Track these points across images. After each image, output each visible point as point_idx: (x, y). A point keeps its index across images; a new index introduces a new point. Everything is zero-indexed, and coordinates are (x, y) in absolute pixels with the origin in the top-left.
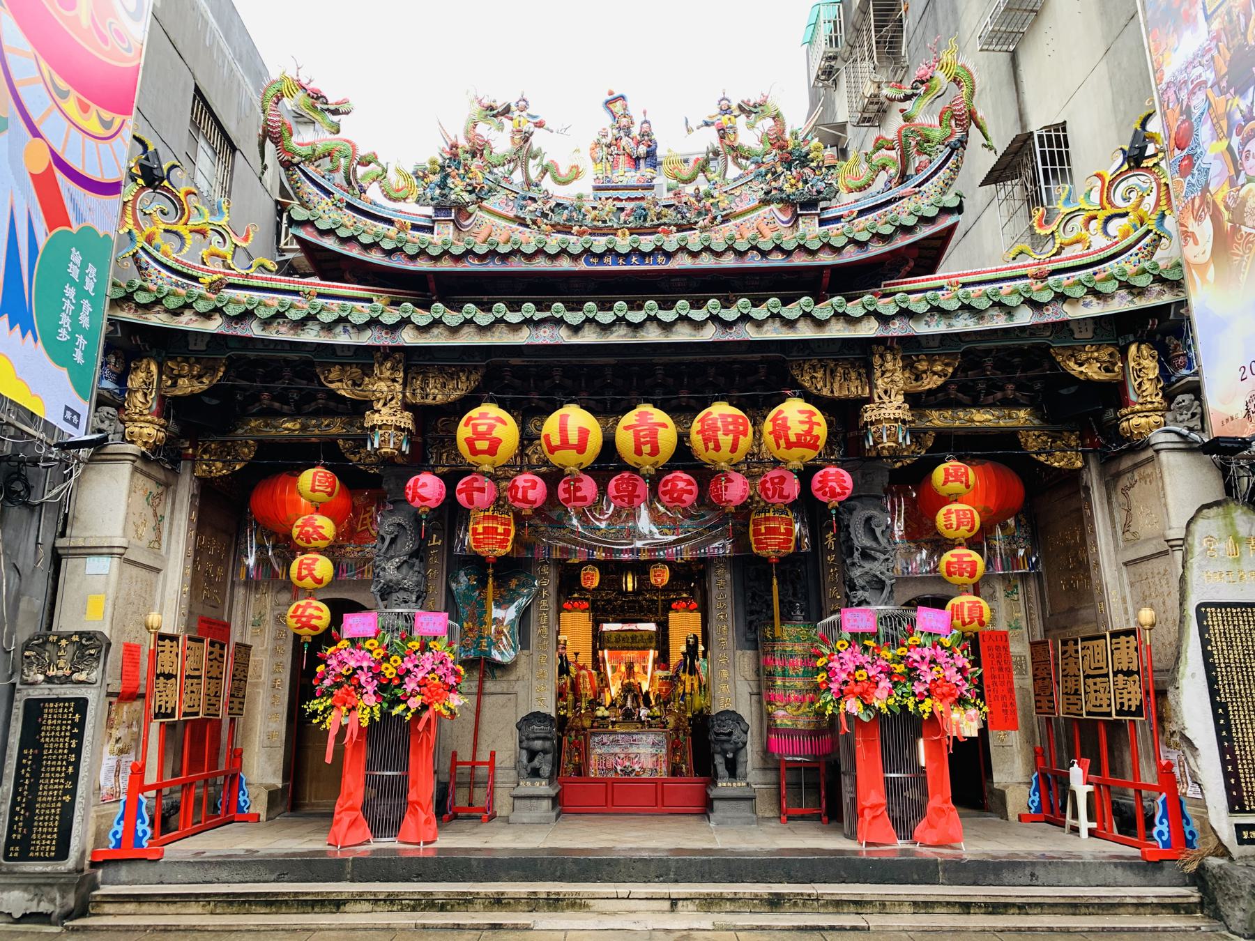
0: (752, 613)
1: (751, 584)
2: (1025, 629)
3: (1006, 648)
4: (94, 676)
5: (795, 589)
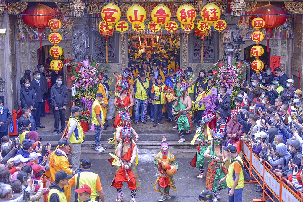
0: (195, 50)
1: (196, 41)
2: (286, 56)
3: (279, 62)
4: (4, 90)
5: (210, 42)
